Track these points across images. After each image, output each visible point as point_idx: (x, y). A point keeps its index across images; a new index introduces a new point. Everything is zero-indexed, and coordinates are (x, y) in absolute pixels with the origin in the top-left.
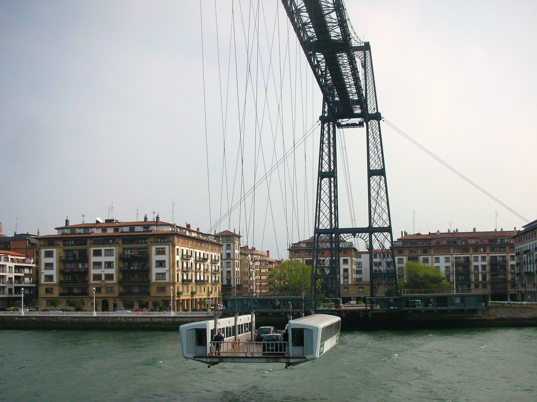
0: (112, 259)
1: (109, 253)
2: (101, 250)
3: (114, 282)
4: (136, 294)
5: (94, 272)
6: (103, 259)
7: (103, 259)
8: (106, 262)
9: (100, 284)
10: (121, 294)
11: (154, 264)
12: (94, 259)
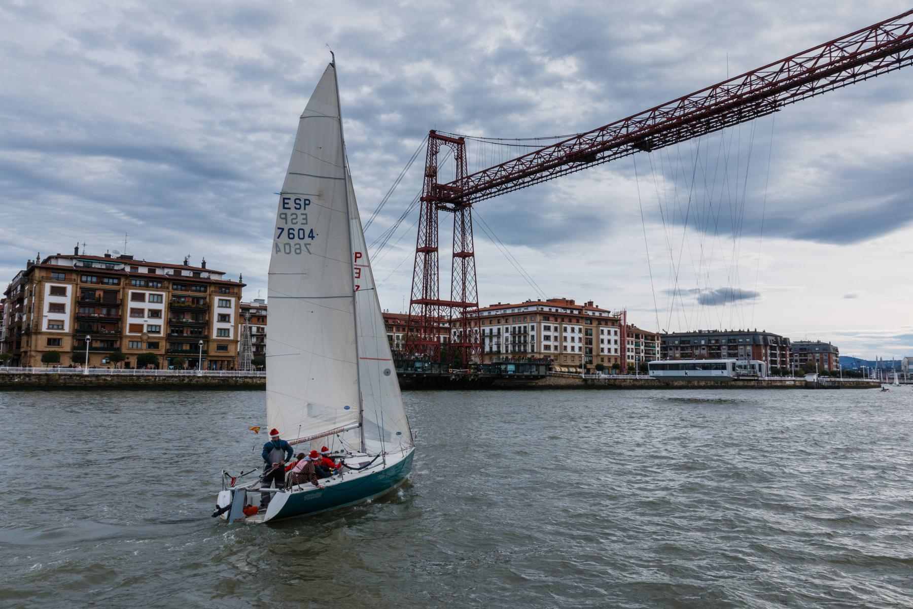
0: (162, 307)
2: (144, 294)
3: (162, 335)
4: (186, 352)
5: (130, 320)
6: (146, 306)
7: (146, 306)
8: (149, 310)
9: (141, 337)
10: (167, 351)
11: (216, 317)
12: (132, 304)
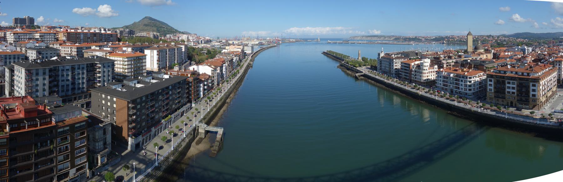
0: (515, 86)
1: (513, 84)
5: (507, 90)
6: (511, 86)
7: (511, 86)
12: (507, 85)
